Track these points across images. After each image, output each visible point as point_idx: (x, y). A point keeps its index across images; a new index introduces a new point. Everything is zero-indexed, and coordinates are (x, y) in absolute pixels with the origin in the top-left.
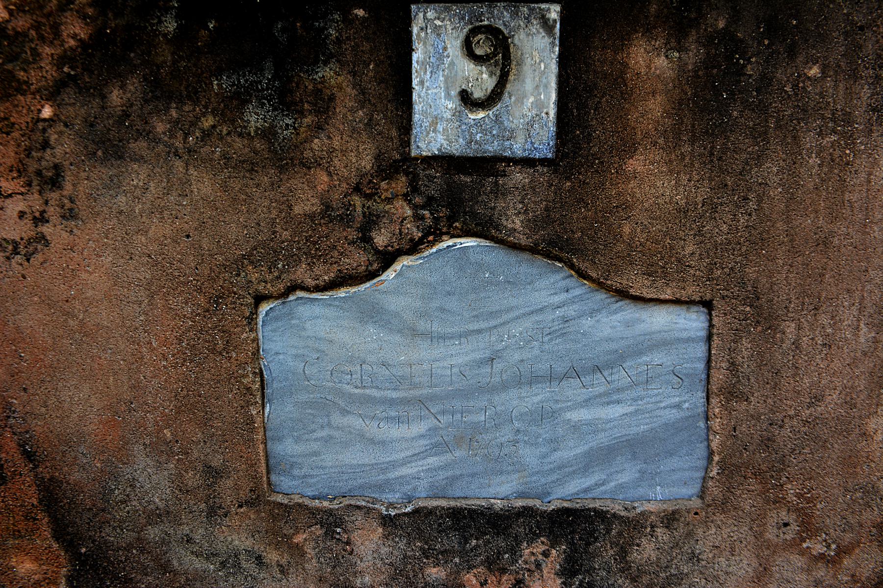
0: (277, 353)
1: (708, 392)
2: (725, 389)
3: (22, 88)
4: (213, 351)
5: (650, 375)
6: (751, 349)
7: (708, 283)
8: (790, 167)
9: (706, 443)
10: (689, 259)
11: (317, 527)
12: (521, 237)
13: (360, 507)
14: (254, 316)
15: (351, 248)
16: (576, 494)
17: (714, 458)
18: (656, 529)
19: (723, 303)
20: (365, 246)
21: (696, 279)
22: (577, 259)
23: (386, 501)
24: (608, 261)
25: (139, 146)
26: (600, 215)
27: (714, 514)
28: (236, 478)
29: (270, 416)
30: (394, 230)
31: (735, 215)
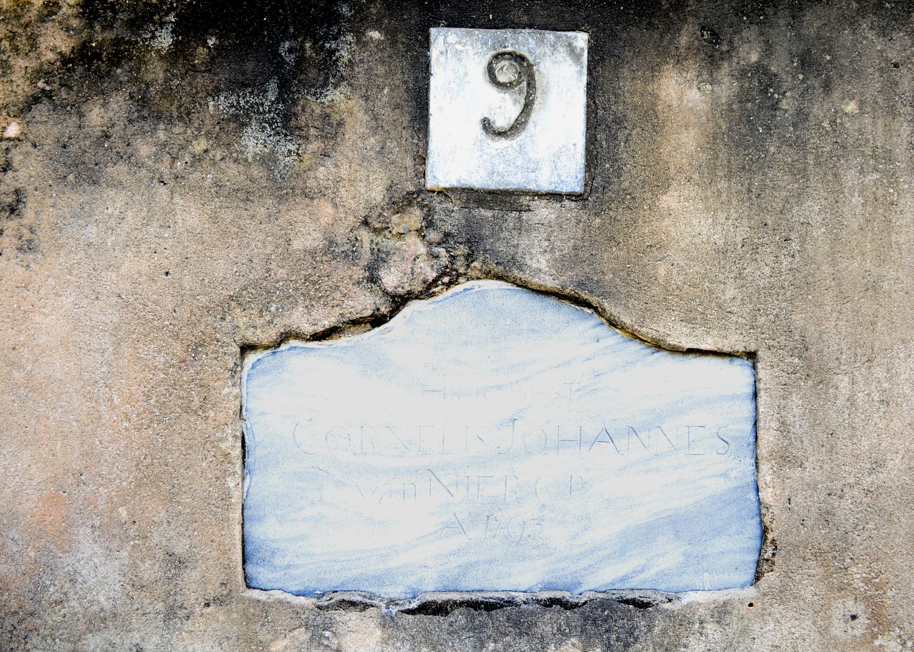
0: (263, 413)
1: (757, 458)
2: (776, 453)
4: (187, 410)
5: (691, 439)
6: (802, 406)
7: (752, 331)
8: (832, 206)
9: (758, 519)
10: (730, 305)
11: (301, 630)
12: (547, 278)
13: (355, 602)
14: (239, 369)
15: (356, 289)
16: (612, 583)
17: (768, 535)
18: (705, 625)
19: (769, 353)
20: (372, 287)
21: (739, 327)
22: (609, 303)
23: (386, 597)
24: (642, 305)
25: (120, 171)
26: (633, 255)
27: (771, 605)
28: (204, 569)
29: (250, 491)
30: (405, 269)
31: (777, 257)
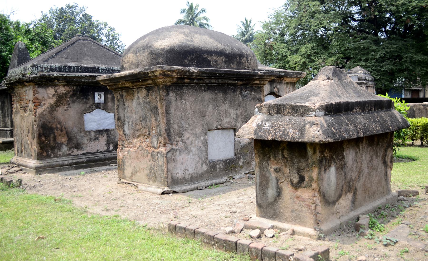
3: (67, 97)
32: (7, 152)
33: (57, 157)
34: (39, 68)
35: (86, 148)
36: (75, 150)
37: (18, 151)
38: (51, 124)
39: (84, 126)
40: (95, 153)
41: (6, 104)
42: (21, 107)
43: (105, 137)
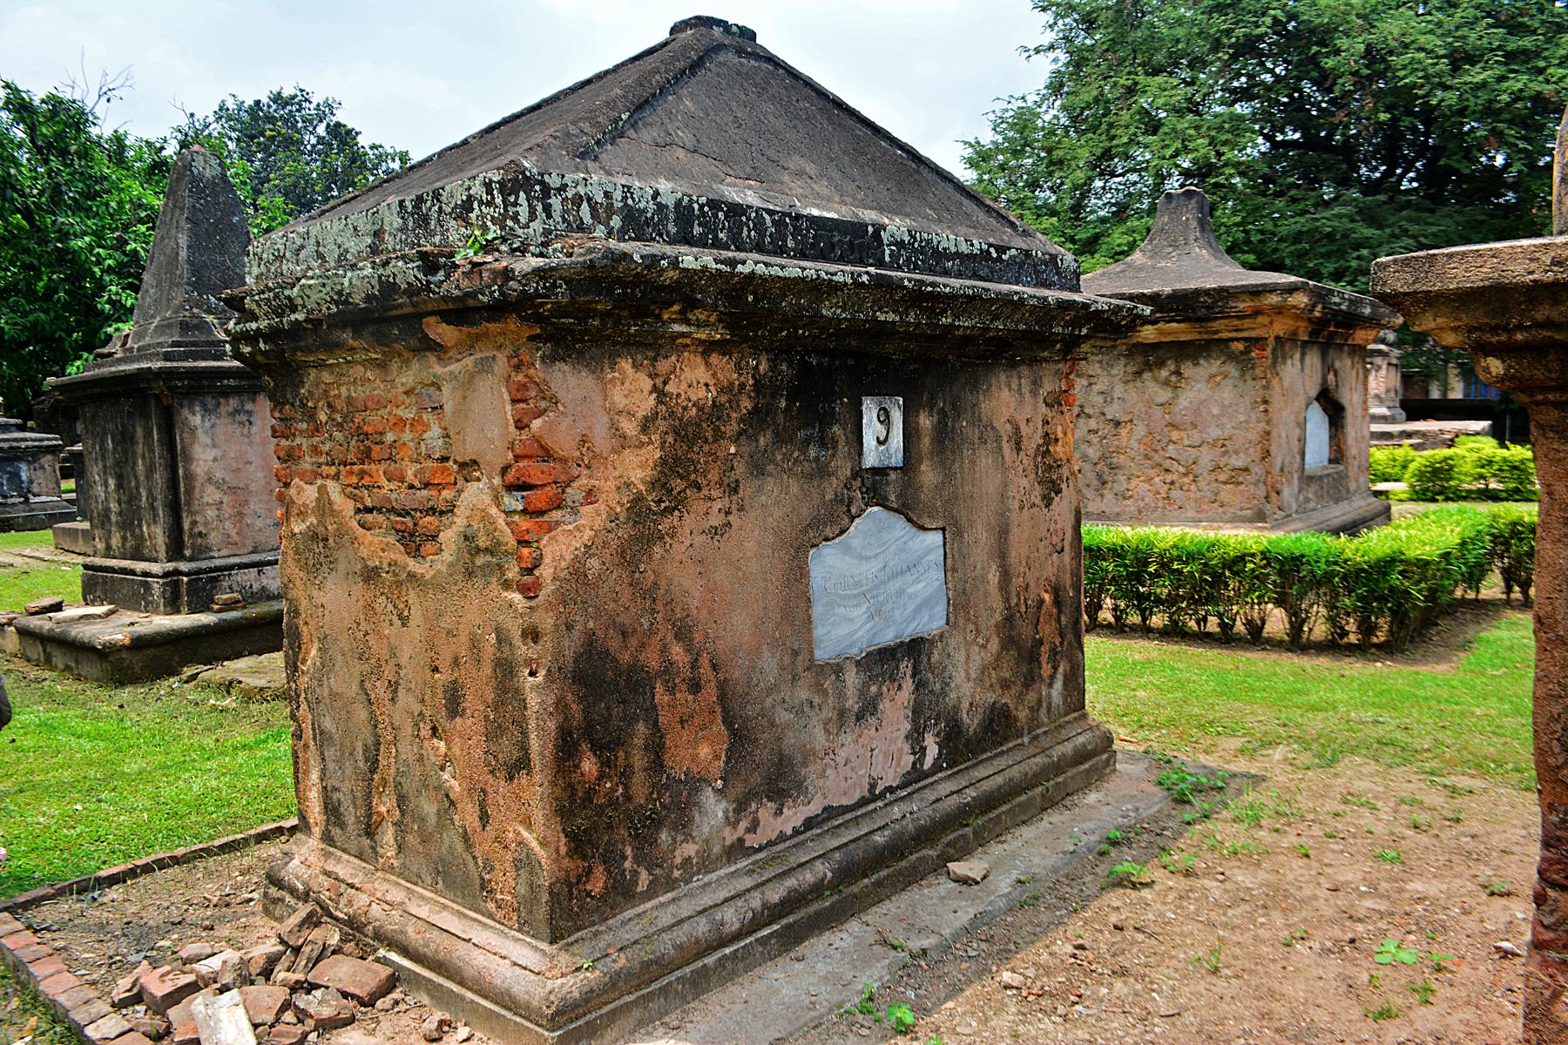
25: (770, 468)
32: (164, 686)
33: (671, 884)
34: (555, 202)
35: (820, 782)
36: (765, 811)
37: (332, 810)
38: (633, 642)
39: (810, 630)
40: (863, 802)
41: (140, 449)
42: (369, 510)
43: (906, 693)
